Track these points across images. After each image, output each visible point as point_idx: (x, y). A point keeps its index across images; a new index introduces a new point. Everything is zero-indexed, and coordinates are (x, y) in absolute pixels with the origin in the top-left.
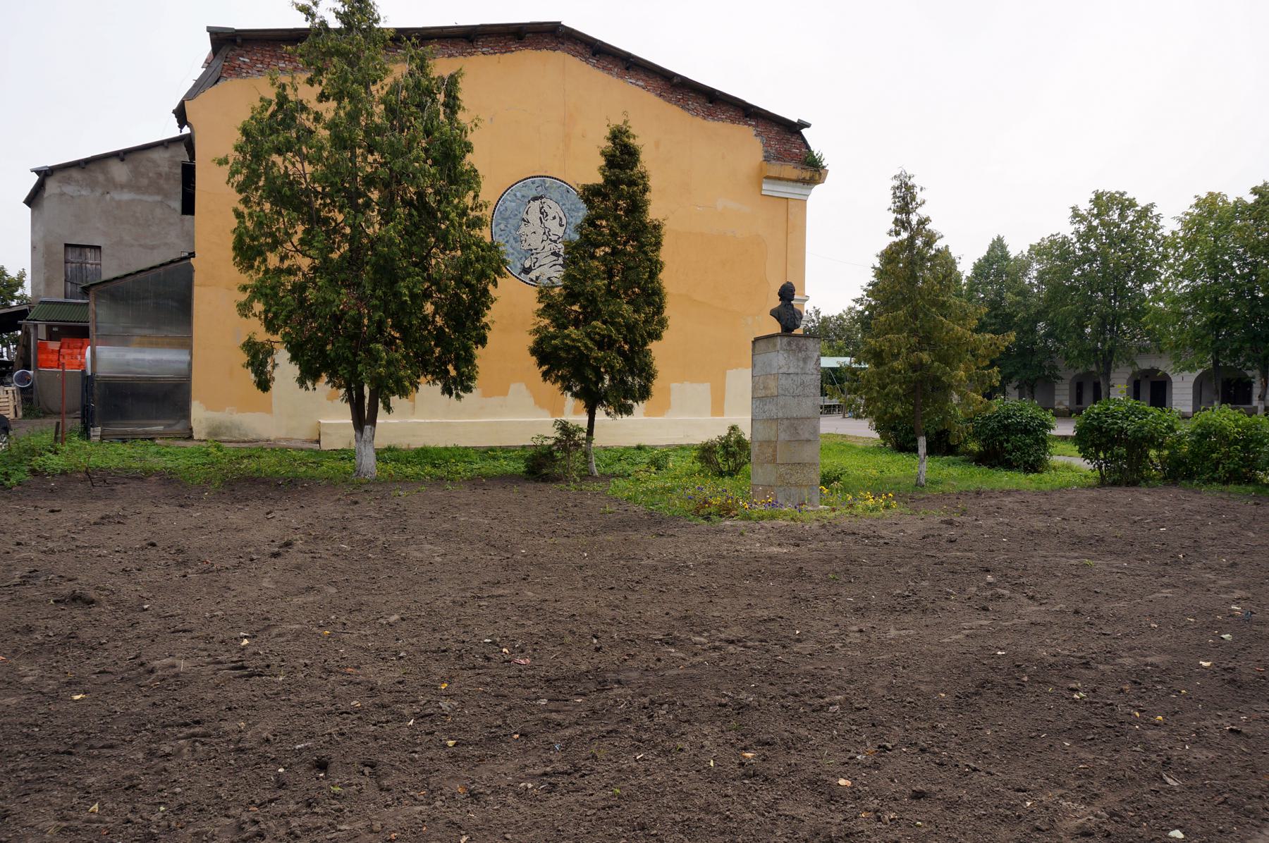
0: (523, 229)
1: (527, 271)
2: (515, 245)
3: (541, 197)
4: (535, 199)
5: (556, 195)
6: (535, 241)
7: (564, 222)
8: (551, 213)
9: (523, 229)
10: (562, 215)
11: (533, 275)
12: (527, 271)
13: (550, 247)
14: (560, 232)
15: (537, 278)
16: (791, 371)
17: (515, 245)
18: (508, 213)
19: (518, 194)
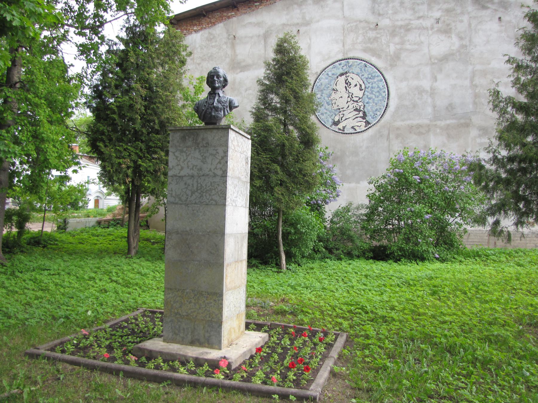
0: (333, 96)
1: (336, 123)
2: (327, 107)
3: (346, 73)
4: (342, 75)
5: (357, 70)
6: (342, 103)
7: (363, 87)
8: (353, 83)
9: (333, 96)
10: (361, 83)
11: (340, 126)
12: (336, 123)
13: (352, 105)
14: (360, 94)
15: (344, 128)
16: (182, 173)
17: (327, 107)
18: (323, 86)
19: (330, 74)
